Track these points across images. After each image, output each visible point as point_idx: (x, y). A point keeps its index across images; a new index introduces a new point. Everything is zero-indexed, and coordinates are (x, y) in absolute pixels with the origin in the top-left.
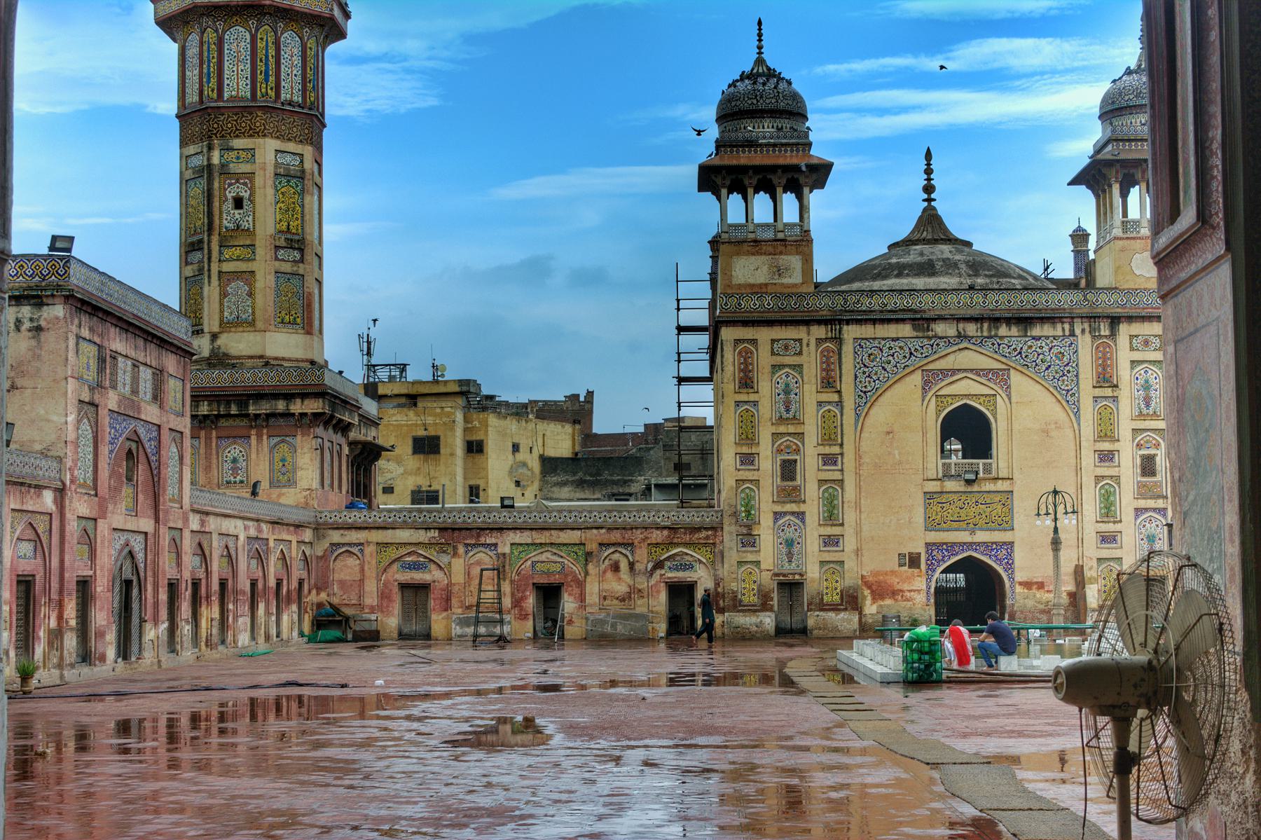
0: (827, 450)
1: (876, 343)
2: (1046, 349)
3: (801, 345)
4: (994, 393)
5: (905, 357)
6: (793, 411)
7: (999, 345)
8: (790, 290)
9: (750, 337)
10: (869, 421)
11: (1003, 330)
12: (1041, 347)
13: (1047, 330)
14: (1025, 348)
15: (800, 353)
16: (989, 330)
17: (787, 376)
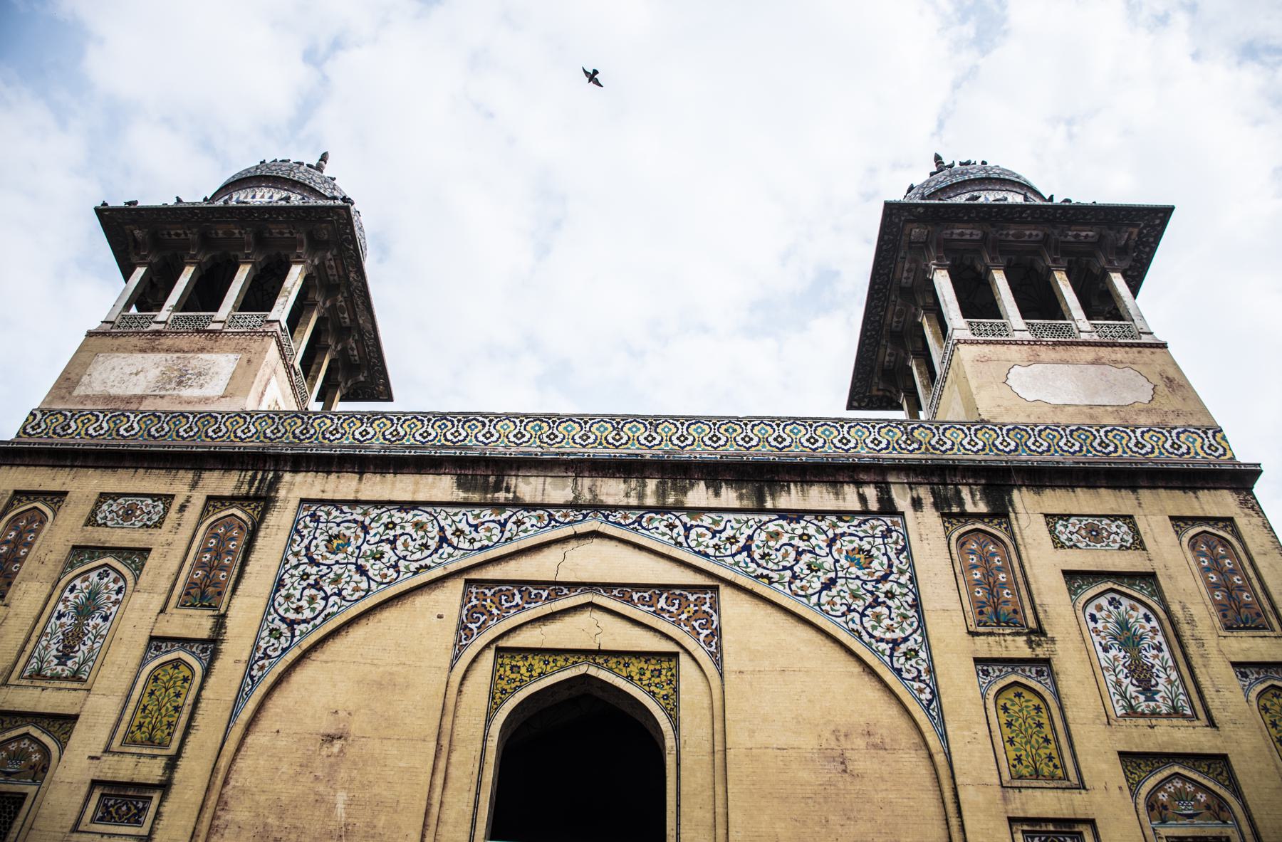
0: (126, 768)
1: (357, 514)
2: (820, 540)
3: (166, 510)
4: (670, 647)
5: (426, 546)
6: (82, 651)
7: (688, 529)
8: (190, 408)
9: (55, 486)
10: (280, 701)
11: (699, 495)
12: (805, 537)
13: (818, 497)
14: (760, 538)
15: (158, 525)
16: (661, 493)
17: (101, 577)
